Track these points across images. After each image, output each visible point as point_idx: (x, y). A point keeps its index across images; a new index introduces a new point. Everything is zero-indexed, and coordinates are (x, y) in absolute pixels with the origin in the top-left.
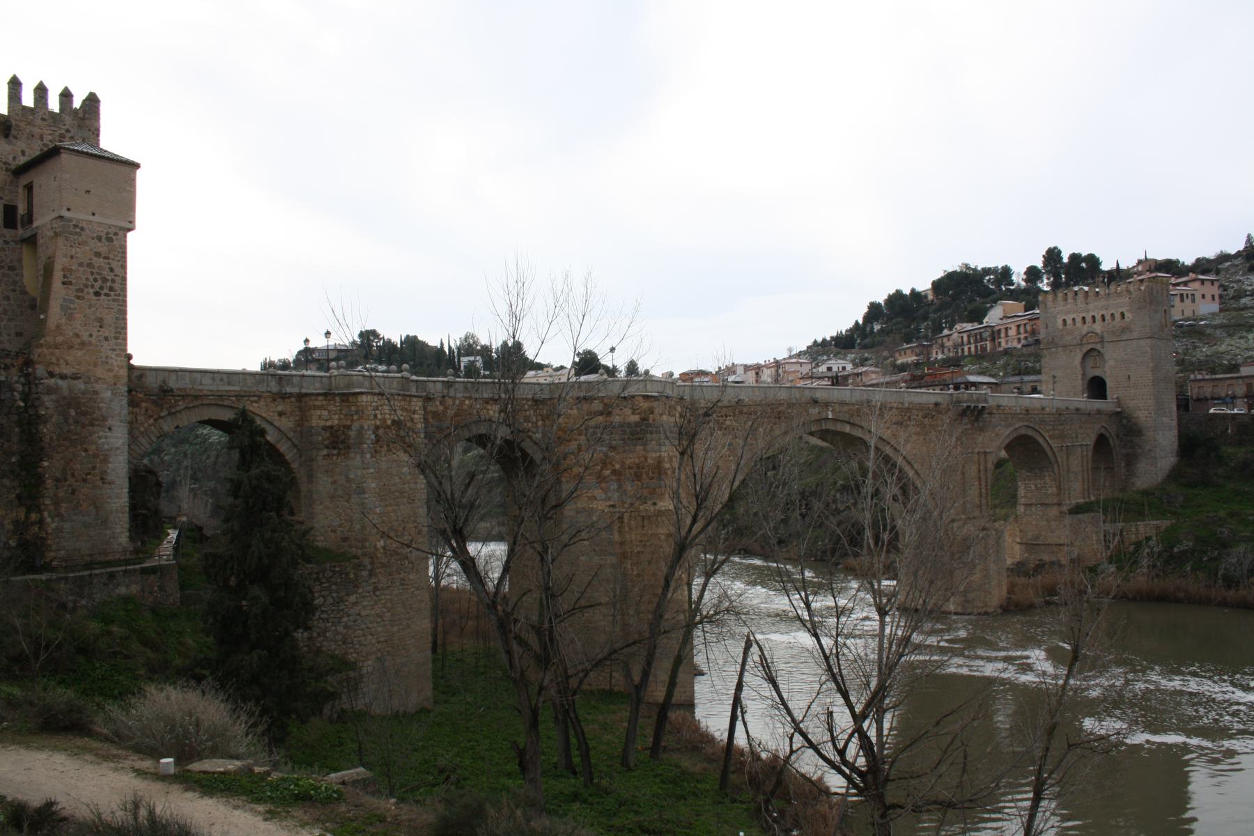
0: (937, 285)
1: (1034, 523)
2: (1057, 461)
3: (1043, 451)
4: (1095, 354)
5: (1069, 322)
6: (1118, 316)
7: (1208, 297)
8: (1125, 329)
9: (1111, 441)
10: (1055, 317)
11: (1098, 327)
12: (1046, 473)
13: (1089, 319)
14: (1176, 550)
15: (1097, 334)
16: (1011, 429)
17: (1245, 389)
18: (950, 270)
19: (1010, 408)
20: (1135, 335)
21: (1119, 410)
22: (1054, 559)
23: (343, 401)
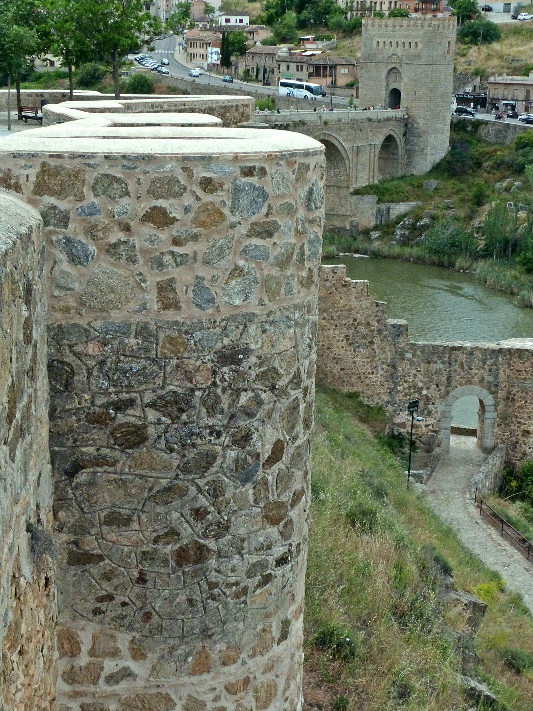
1: (331, 199)
2: (348, 157)
3: (338, 151)
5: (381, 44)
6: (413, 45)
8: (417, 56)
9: (398, 140)
10: (372, 39)
11: (399, 51)
12: (341, 165)
14: (418, 224)
15: (398, 56)
19: (312, 122)
20: (423, 61)
21: (406, 117)
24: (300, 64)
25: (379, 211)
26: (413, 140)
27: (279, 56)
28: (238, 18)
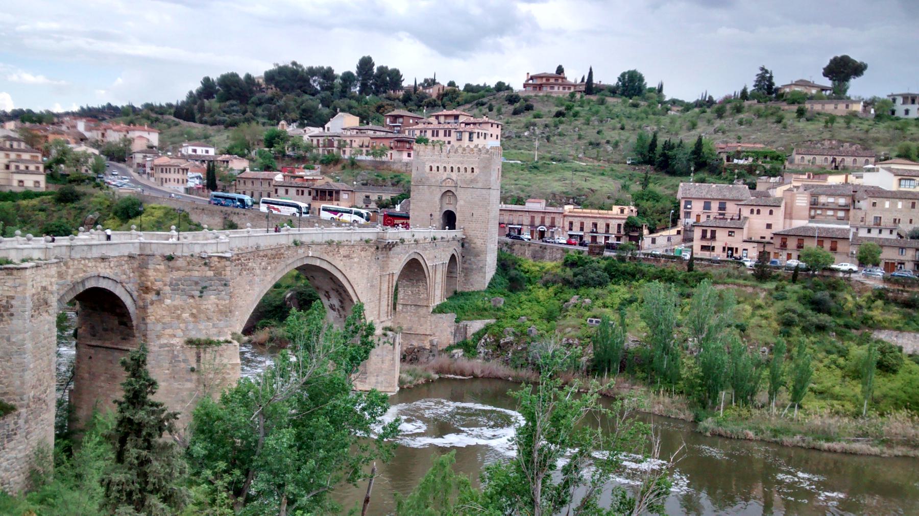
0: (270, 77)
4: (450, 194)
5: (434, 169)
6: (469, 170)
7: (494, 136)
8: (472, 181)
10: (424, 163)
11: (454, 176)
13: (449, 169)
16: (407, 255)
17: (530, 219)
18: (281, 65)
20: (480, 185)
21: (464, 237)
22: (421, 344)
23: (8, 274)
24: (300, 189)
25: (457, 330)
26: (470, 260)
27: (277, 182)
28: (204, 149)
